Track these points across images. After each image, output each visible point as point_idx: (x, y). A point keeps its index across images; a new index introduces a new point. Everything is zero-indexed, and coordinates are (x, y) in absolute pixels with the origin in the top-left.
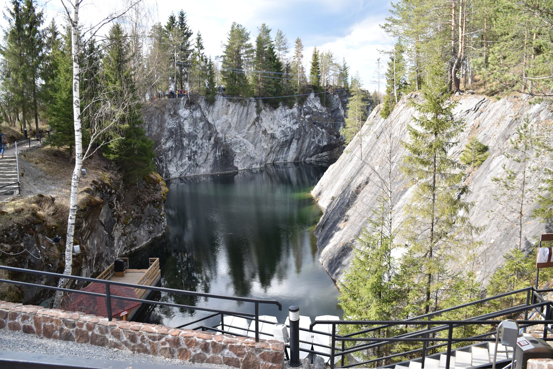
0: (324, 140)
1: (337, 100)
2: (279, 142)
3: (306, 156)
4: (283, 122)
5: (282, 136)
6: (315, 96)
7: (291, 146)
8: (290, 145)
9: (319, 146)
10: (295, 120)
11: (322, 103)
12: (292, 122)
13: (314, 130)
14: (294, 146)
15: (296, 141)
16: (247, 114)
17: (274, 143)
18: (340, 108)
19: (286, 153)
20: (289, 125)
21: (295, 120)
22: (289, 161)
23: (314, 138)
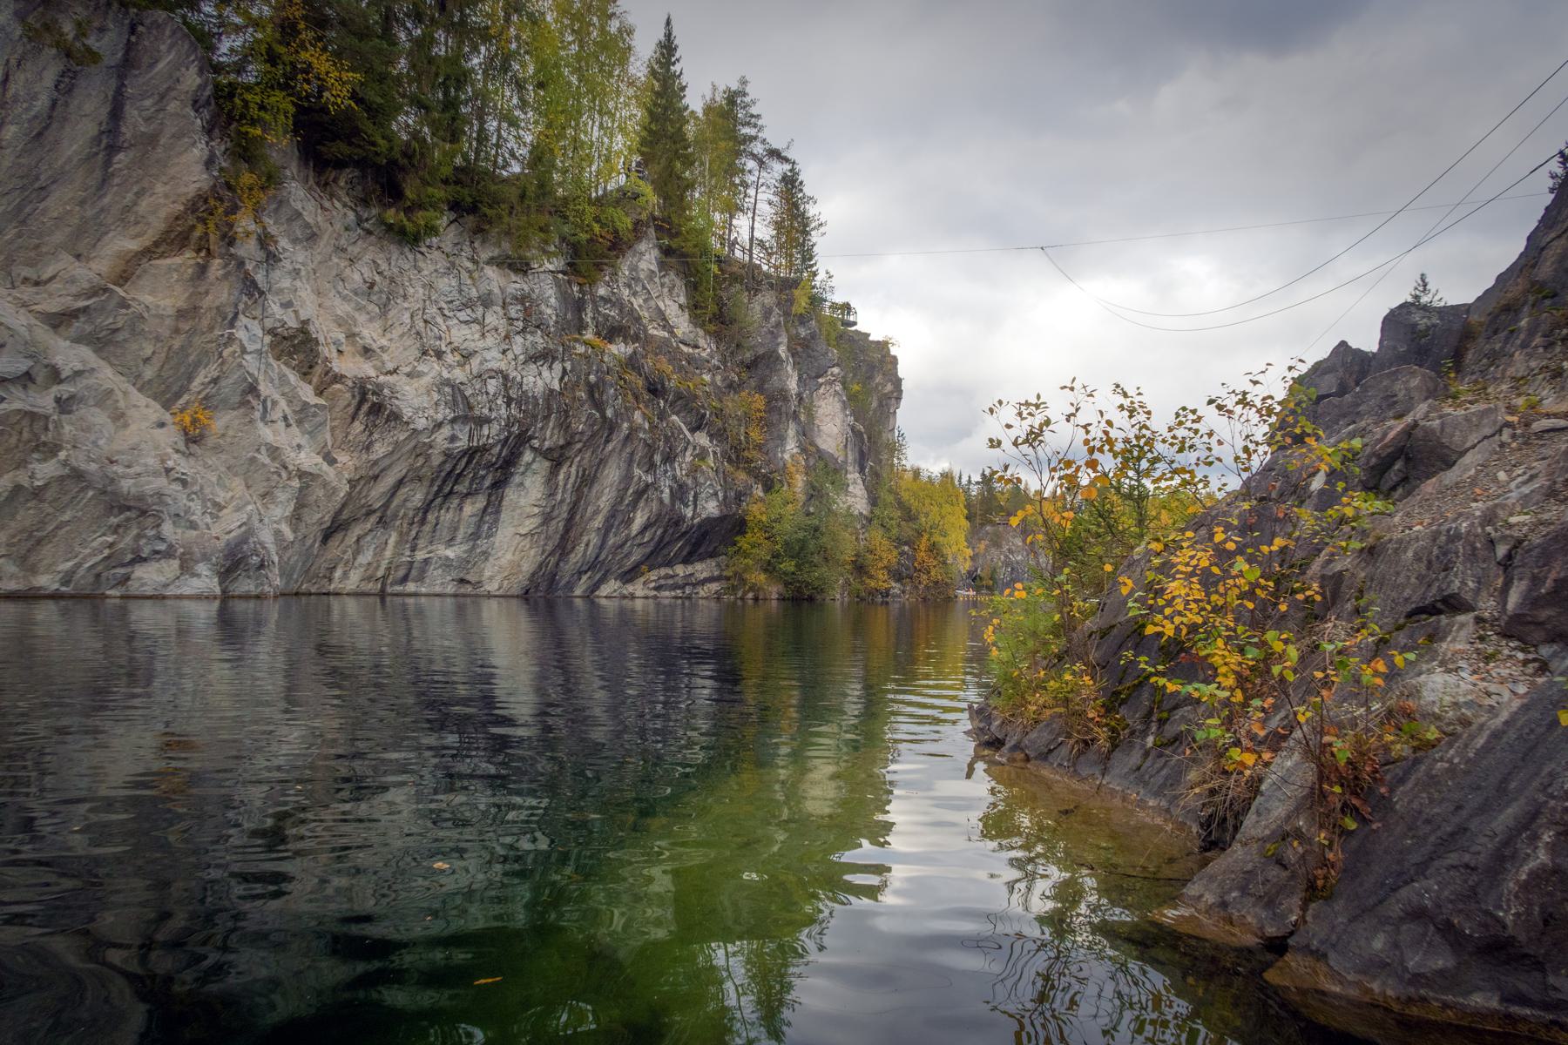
0: (706, 491)
1: (767, 313)
2: (422, 451)
3: (598, 568)
4: (461, 334)
5: (444, 413)
6: (662, 265)
7: (511, 494)
8: (499, 485)
9: (680, 520)
10: (539, 340)
11: (694, 308)
12: (518, 349)
13: (653, 427)
14: (528, 492)
15: (543, 466)
16: (110, 141)
17: (380, 450)
18: (782, 351)
19: (475, 536)
20: (495, 360)
21: (539, 340)
22: (492, 587)
23: (651, 467)
